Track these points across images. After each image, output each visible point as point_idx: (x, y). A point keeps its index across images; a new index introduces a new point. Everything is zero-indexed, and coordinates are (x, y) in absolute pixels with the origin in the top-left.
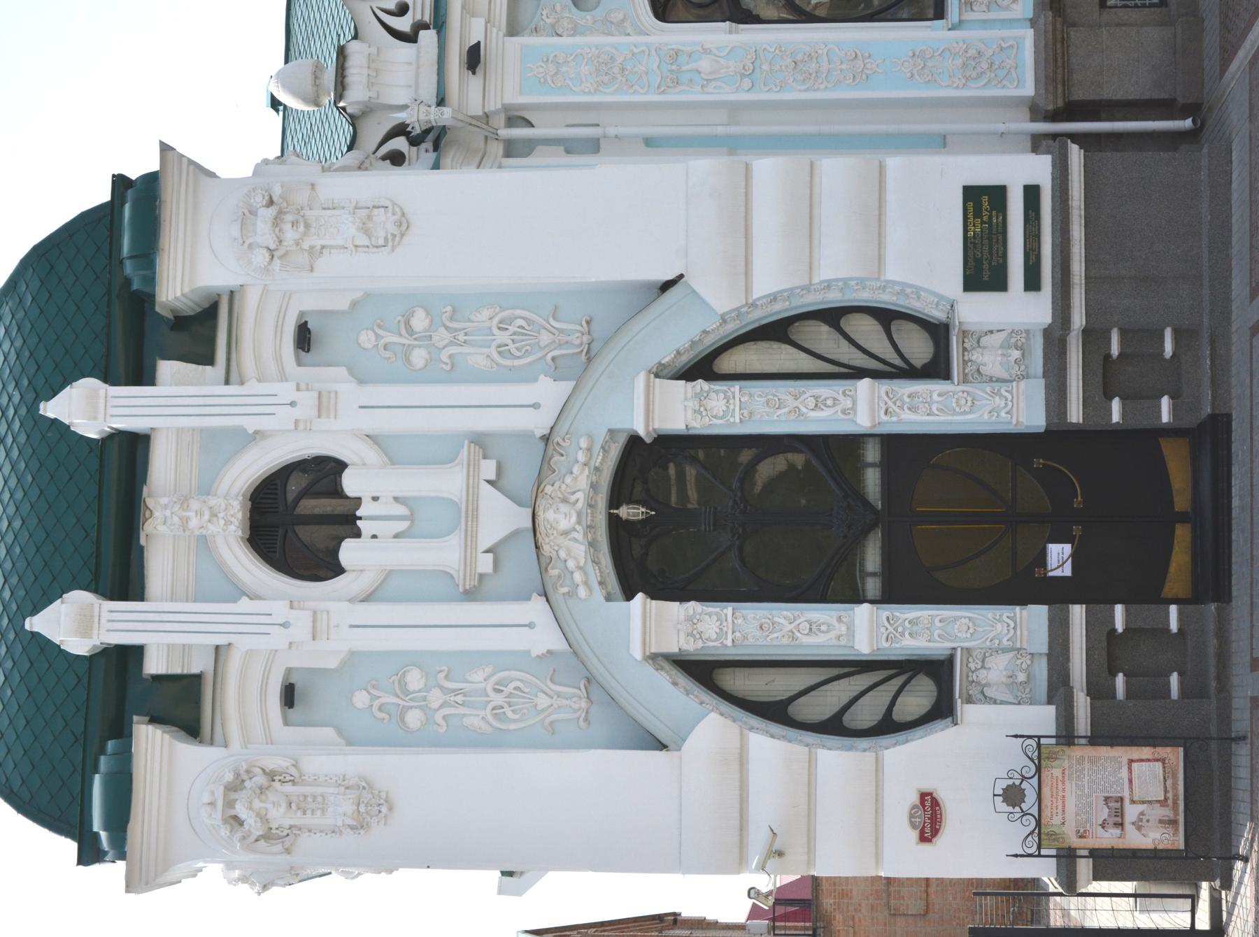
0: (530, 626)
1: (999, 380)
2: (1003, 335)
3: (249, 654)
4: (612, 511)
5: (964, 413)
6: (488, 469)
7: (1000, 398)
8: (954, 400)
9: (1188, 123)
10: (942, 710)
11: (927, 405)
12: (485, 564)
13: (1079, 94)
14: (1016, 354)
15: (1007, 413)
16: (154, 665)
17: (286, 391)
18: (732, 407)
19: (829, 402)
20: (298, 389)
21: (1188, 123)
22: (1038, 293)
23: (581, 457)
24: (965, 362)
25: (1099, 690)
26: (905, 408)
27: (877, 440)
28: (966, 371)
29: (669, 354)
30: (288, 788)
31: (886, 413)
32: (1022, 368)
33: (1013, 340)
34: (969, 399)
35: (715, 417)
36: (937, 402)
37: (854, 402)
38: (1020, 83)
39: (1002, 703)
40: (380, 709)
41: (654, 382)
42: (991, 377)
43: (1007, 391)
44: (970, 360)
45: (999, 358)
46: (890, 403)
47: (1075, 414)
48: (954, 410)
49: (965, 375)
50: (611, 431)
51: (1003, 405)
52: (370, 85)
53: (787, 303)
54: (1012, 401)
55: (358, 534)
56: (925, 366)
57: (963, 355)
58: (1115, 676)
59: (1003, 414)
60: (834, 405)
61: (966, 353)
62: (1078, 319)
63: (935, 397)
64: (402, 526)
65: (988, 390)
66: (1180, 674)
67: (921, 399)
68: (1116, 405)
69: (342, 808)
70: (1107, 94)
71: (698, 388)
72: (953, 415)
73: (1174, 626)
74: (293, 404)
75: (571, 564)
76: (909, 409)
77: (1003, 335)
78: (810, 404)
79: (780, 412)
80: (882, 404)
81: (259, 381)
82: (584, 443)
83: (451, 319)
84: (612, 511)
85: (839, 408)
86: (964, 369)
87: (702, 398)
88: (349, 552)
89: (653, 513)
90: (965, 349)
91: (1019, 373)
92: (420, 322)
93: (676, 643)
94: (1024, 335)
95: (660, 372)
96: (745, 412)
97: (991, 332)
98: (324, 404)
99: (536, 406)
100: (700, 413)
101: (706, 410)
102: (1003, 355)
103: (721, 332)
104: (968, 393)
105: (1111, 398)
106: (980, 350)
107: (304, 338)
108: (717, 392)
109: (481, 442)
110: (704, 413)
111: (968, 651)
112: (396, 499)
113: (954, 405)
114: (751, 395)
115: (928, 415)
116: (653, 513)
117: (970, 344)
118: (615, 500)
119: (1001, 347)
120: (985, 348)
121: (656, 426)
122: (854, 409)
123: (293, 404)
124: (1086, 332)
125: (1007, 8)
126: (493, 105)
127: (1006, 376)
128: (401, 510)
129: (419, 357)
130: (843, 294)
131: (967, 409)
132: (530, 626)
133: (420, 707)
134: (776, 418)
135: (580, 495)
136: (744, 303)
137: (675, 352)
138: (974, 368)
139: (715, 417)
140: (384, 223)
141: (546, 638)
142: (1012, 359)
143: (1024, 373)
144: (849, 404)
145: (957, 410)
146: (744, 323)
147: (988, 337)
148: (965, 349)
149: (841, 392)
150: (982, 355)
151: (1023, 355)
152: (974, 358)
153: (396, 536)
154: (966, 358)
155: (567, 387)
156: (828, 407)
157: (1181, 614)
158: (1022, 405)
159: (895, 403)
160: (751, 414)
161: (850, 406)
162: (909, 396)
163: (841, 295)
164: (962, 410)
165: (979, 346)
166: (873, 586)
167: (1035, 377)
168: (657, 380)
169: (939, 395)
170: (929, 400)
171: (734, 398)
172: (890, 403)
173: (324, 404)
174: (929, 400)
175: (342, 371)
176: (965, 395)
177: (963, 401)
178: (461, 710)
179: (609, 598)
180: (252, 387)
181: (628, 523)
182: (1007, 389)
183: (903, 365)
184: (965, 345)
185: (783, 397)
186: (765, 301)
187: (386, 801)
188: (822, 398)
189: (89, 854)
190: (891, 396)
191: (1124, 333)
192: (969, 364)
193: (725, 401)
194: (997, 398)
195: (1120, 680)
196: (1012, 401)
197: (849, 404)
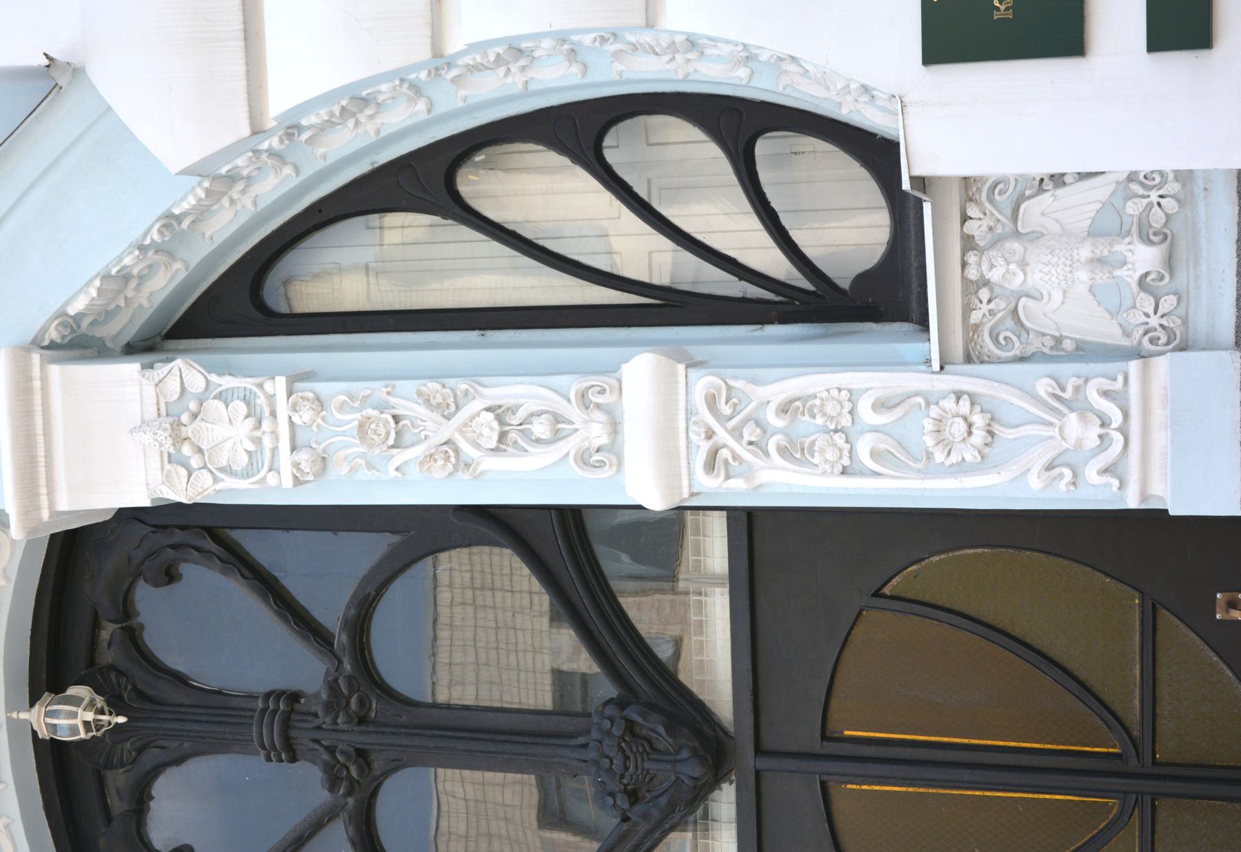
1: (1085, 352)
2: (1098, 191)
4: (14, 715)
5: (962, 468)
7: (1083, 418)
8: (929, 425)
11: (839, 439)
14: (1145, 257)
15: (1106, 471)
18: (267, 442)
19: (540, 428)
22: (1203, 54)
24: (971, 288)
26: (772, 448)
27: (725, 513)
28: (975, 317)
29: (88, 284)
31: (711, 465)
32: (1168, 303)
33: (1133, 208)
34: (978, 420)
35: (228, 470)
36: (875, 430)
37: (615, 427)
41: (44, 379)
42: (1058, 340)
43: (1105, 394)
44: (987, 283)
45: (1083, 275)
46: (722, 435)
48: (929, 456)
49: (972, 330)
51: (1092, 440)
53: (421, 106)
54: (1124, 431)
56: (863, 279)
57: (964, 265)
59: (1091, 473)
60: (557, 436)
61: (972, 258)
63: (866, 413)
65: (1043, 387)
67: (820, 420)
71: (173, 385)
72: (924, 474)
76: (783, 451)
77: (1098, 191)
78: (486, 432)
79: (401, 456)
80: (698, 439)
84: (14, 715)
85: (569, 446)
86: (967, 310)
87: (185, 418)
89: (121, 720)
90: (968, 243)
91: (1154, 321)
94: (1173, 187)
96: (303, 457)
97: (1058, 180)
100: (185, 464)
101: (200, 451)
102: (1098, 262)
103: (247, 201)
104: (974, 400)
106: (1016, 246)
108: (224, 397)
110: (195, 462)
113: (929, 441)
114: (320, 403)
115: (844, 472)
116: (121, 720)
117: (987, 222)
119: (1093, 233)
120: (1035, 237)
121: (63, 505)
122: (614, 448)
127: (1107, 331)
130: (585, 68)
131: (970, 456)
134: (393, 474)
136: (246, 131)
137: (97, 283)
138: (1000, 305)
139: (228, 470)
142: (1130, 276)
143: (1173, 323)
144: (597, 434)
145: (939, 457)
146: (307, 172)
147: (1046, 198)
148: (968, 243)
149: (572, 397)
150: (1023, 265)
151: (1170, 262)
152: (995, 276)
154: (972, 274)
156: (538, 441)
158: (1160, 439)
159: (737, 433)
160: (323, 461)
161: (604, 440)
162: (784, 409)
163: (575, 69)
164: (954, 458)
165: (1017, 234)
167: (1211, 345)
168: (55, 370)
169: (881, 406)
170: (846, 421)
171: (273, 414)
172: (722, 435)
174: (846, 421)
176: (965, 406)
177: (959, 427)
182: (1106, 384)
184: (971, 227)
185: (405, 407)
186: (323, 114)
188: (521, 414)
190: (726, 410)
192: (984, 294)
193: (251, 422)
194: (1073, 417)
196: (1124, 431)
197: (597, 434)
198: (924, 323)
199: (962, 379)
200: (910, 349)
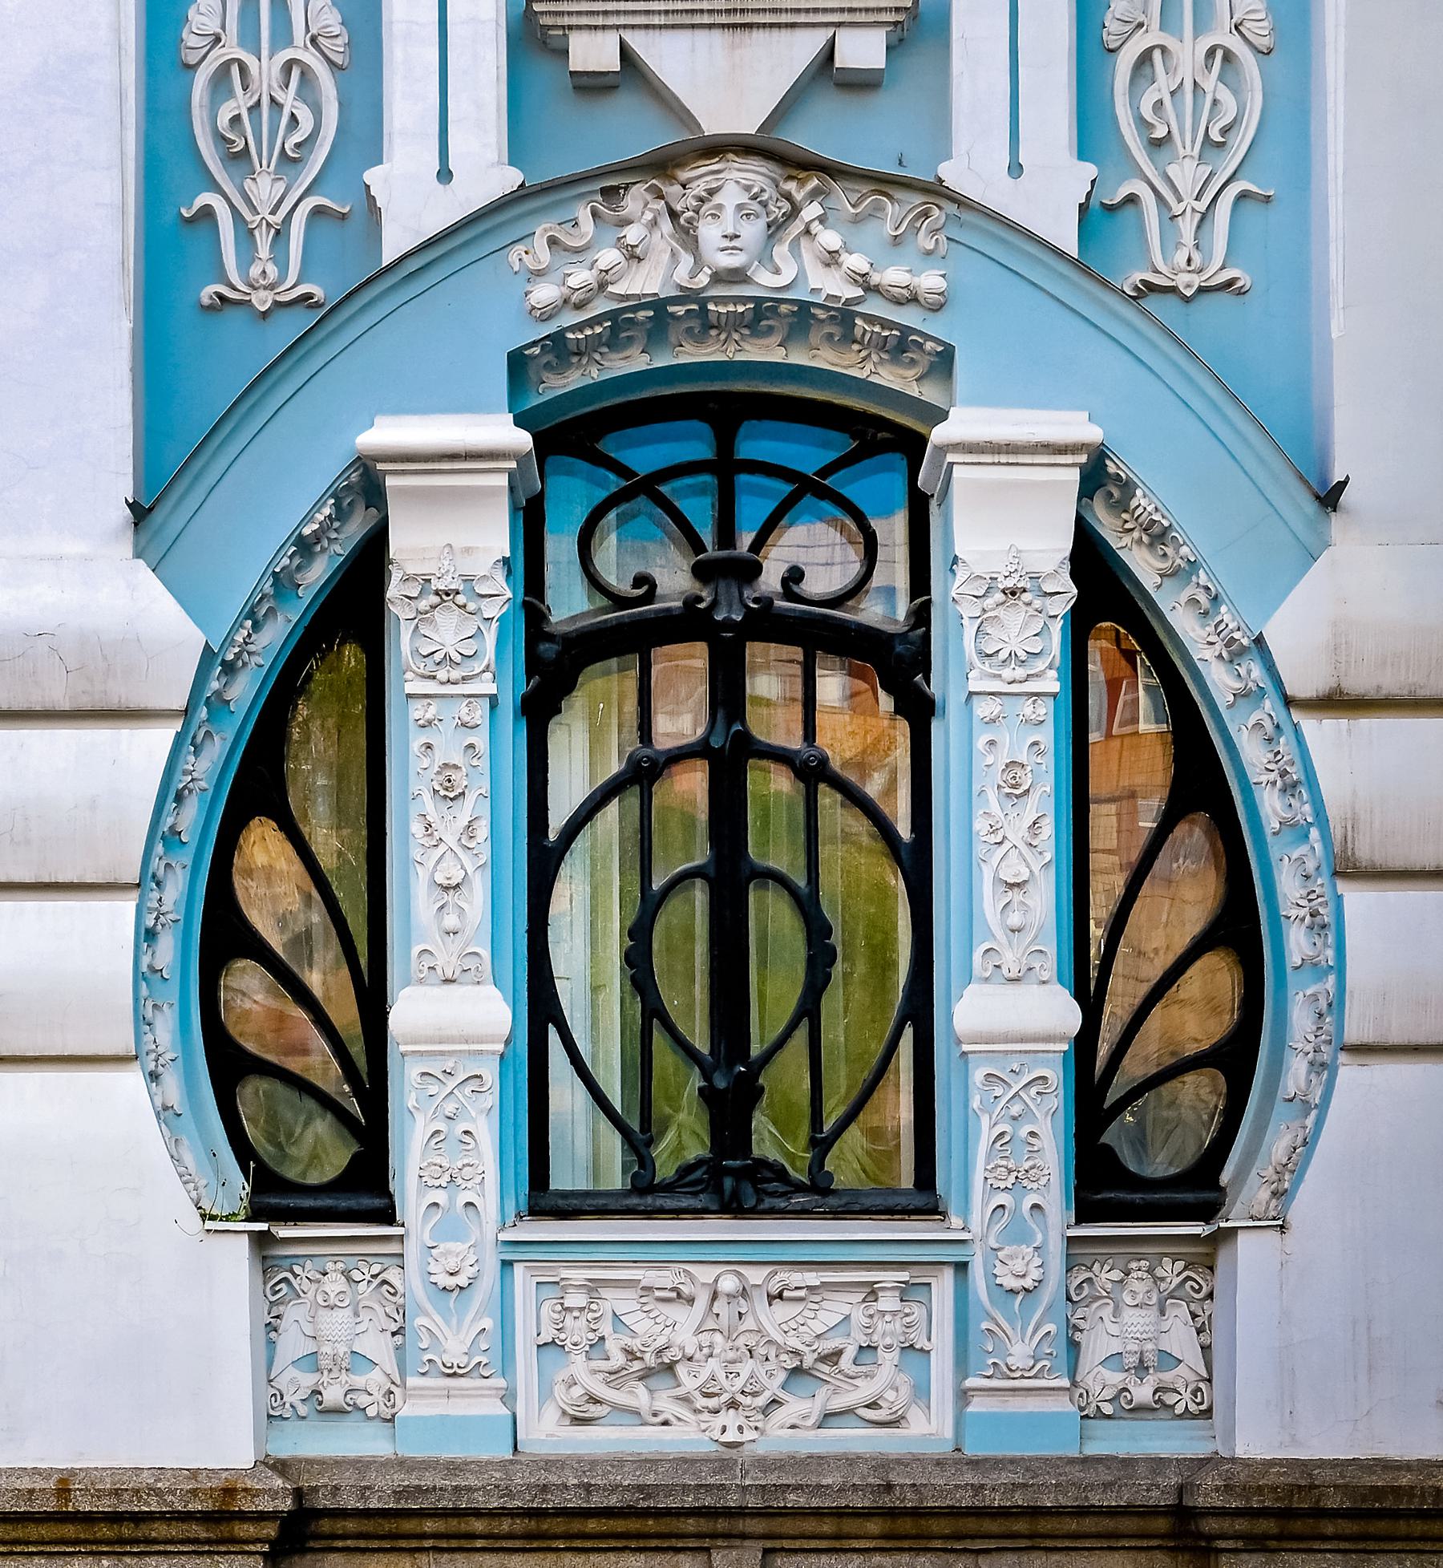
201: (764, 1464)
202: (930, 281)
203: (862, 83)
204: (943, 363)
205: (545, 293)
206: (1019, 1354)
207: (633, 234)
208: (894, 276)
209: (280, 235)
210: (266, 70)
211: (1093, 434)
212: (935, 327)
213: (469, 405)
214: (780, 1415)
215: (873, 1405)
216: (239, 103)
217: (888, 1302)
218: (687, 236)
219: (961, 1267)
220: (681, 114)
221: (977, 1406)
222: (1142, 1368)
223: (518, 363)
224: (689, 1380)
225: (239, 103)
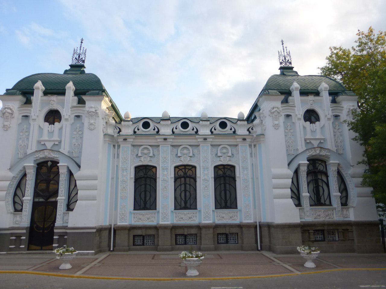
0: (31, 149)
3: (31, 110)
6: (57, 143)
9: (112, 249)
10: (16, 210)
12: (43, 143)
13: (117, 232)
16: (32, 97)
17: (69, 113)
20: (69, 116)
21: (112, 249)
23: (55, 156)
25: (12, 235)
30: (10, 116)
38: (120, 222)
39: (13, 220)
40: (24, 129)
47: (55, 231)
50: (59, 160)
52: (125, 125)
55: (50, 125)
58: (15, 237)
62: (68, 231)
64: (50, 131)
66: (14, 248)
68: (57, 237)
69: (6, 123)
70: (117, 236)
73: (21, 246)
74: (67, 115)
75: (39, 155)
81: (71, 110)
82: (57, 156)
83: (80, 137)
88: (47, 124)
92: (80, 133)
93: (27, 171)
95: (68, 168)
98: (67, 120)
99: (64, 149)
105: (59, 236)
107: (78, 117)
109: (60, 142)
111: (21, 214)
112: (53, 131)
118: (51, 161)
123: (67, 115)
124: (67, 232)
125: (134, 220)
126: (120, 143)
128: (52, 131)
129: (75, 133)
132: (31, 149)
133: (23, 135)
135: (49, 156)
140: (92, 127)
141: (29, 152)
153: (48, 130)
155: (67, 154)
157: (23, 248)
166: (37, 200)
173: (67, 120)
175: (73, 121)
178: (22, 141)
179: (35, 161)
180: (70, 109)
181: (47, 164)
183: (70, 204)
187: (7, 130)
189: (7, 90)
191: (66, 238)
195: (14, 238)
198: (67, 211)
199: (62, 213)
200: (65, 211)
201: (327, 221)
202: (329, 154)
203: (322, 143)
204: (329, 158)
205: (308, 154)
206: (339, 214)
207: (313, 151)
208: (327, 154)
209: (292, 151)
210: (290, 142)
211: (338, 162)
212: (329, 156)
213: (303, 161)
214: (326, 218)
215: (331, 217)
216: (289, 144)
217: (331, 211)
218: (316, 151)
219: (335, 209)
220: (313, 145)
221: (337, 217)
222: (346, 215)
223: (307, 158)
224: (321, 216)
225: (289, 144)
